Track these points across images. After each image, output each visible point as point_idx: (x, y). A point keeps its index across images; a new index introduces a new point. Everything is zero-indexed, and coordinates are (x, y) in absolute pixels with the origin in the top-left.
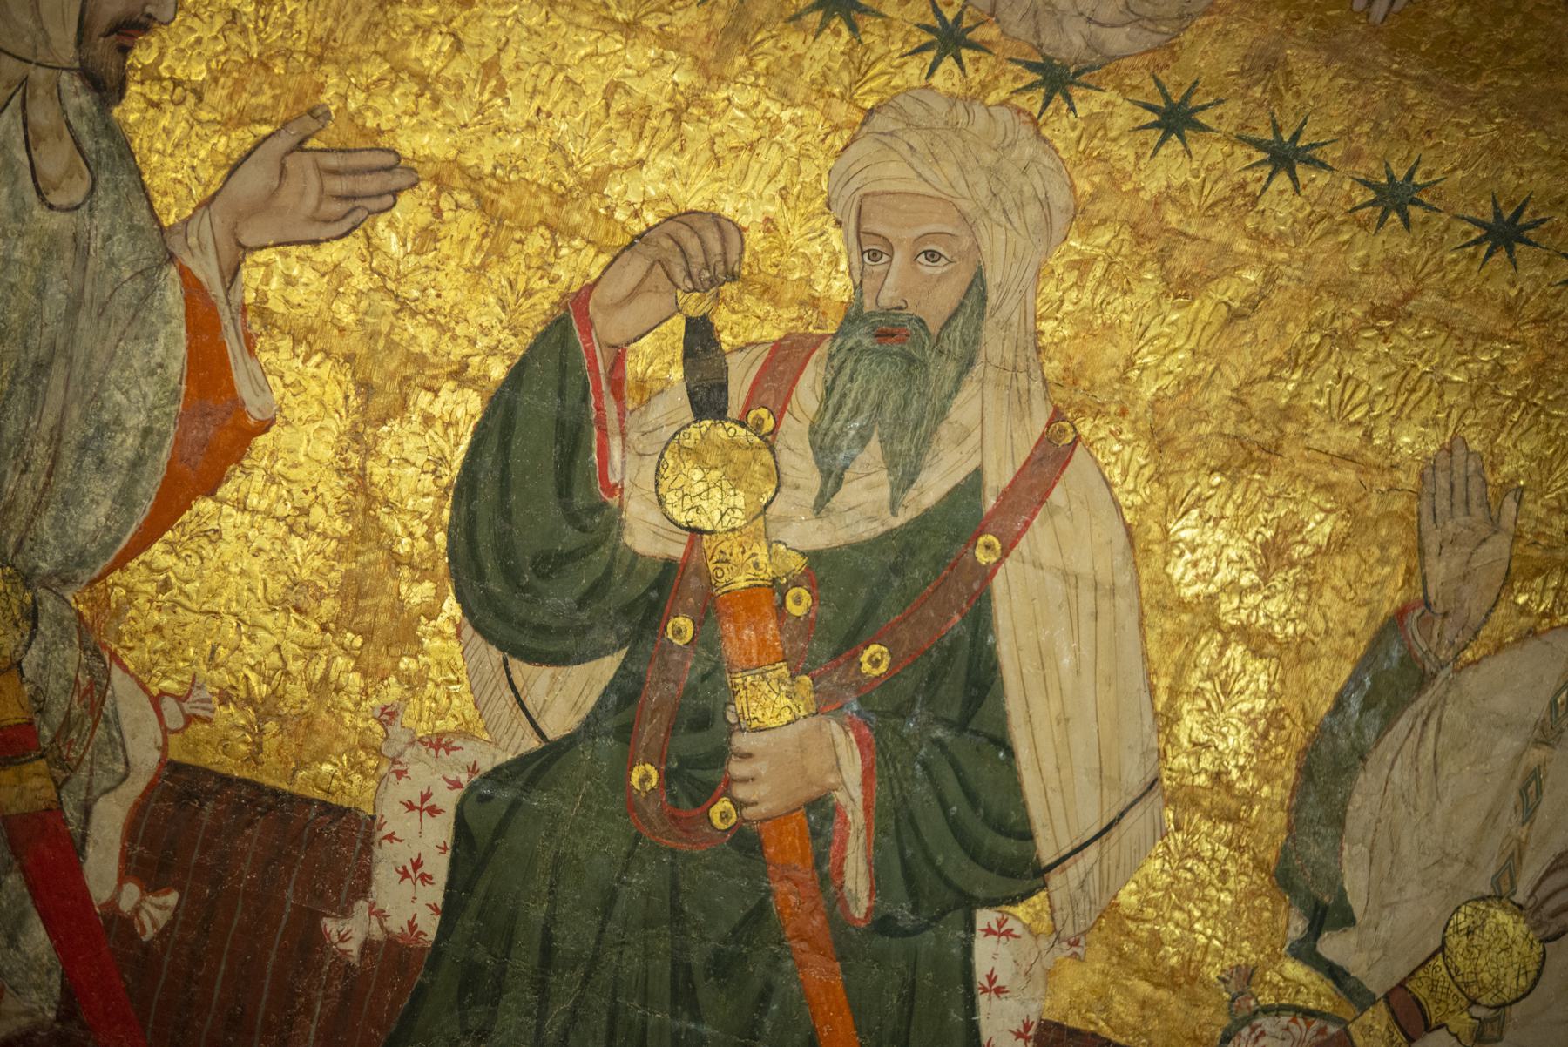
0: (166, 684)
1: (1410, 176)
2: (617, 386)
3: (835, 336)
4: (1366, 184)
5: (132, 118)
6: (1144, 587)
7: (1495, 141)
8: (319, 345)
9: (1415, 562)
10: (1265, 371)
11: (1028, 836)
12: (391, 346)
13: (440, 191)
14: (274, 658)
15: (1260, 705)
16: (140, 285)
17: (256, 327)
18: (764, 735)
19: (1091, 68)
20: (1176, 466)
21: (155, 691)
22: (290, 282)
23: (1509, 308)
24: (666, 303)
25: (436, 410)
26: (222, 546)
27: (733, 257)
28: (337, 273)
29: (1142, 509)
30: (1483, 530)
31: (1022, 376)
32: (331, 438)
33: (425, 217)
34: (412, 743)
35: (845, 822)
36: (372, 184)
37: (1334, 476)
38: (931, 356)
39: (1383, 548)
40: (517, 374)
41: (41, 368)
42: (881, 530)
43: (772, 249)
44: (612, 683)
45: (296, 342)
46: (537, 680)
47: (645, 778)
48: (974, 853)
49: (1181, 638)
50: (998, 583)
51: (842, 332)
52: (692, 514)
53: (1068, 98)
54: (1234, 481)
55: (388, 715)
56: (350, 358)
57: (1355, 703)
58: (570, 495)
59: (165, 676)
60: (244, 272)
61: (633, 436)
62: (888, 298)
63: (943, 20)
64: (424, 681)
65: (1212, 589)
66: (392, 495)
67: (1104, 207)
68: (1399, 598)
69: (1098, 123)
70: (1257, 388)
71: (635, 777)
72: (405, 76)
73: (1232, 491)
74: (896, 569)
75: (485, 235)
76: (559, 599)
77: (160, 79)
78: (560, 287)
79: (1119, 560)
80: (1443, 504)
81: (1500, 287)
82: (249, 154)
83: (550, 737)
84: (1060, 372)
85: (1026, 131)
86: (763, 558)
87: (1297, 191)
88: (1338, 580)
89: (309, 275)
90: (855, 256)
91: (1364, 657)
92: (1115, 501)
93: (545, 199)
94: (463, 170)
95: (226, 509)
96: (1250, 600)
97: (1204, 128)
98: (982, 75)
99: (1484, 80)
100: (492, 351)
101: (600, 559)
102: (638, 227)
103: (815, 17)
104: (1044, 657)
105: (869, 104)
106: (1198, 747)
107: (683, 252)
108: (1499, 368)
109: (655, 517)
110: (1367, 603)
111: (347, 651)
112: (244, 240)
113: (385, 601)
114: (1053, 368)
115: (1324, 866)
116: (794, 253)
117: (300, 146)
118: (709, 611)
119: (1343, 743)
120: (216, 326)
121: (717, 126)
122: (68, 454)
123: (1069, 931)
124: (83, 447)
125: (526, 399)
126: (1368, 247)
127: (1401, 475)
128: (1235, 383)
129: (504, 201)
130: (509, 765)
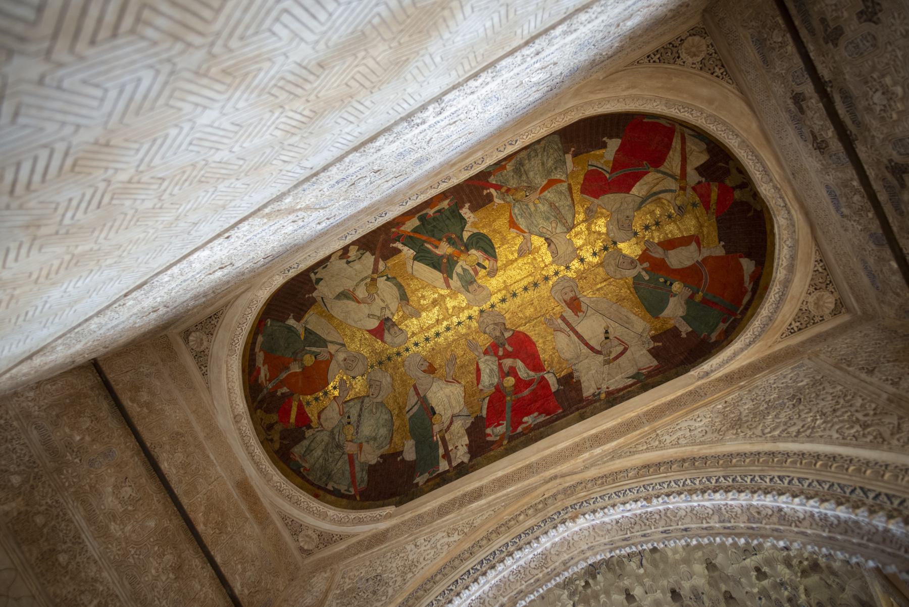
2: (487, 259)
40: (495, 251)
46: (469, 234)
69: (475, 311)
118: (462, 251)
126: (445, 323)
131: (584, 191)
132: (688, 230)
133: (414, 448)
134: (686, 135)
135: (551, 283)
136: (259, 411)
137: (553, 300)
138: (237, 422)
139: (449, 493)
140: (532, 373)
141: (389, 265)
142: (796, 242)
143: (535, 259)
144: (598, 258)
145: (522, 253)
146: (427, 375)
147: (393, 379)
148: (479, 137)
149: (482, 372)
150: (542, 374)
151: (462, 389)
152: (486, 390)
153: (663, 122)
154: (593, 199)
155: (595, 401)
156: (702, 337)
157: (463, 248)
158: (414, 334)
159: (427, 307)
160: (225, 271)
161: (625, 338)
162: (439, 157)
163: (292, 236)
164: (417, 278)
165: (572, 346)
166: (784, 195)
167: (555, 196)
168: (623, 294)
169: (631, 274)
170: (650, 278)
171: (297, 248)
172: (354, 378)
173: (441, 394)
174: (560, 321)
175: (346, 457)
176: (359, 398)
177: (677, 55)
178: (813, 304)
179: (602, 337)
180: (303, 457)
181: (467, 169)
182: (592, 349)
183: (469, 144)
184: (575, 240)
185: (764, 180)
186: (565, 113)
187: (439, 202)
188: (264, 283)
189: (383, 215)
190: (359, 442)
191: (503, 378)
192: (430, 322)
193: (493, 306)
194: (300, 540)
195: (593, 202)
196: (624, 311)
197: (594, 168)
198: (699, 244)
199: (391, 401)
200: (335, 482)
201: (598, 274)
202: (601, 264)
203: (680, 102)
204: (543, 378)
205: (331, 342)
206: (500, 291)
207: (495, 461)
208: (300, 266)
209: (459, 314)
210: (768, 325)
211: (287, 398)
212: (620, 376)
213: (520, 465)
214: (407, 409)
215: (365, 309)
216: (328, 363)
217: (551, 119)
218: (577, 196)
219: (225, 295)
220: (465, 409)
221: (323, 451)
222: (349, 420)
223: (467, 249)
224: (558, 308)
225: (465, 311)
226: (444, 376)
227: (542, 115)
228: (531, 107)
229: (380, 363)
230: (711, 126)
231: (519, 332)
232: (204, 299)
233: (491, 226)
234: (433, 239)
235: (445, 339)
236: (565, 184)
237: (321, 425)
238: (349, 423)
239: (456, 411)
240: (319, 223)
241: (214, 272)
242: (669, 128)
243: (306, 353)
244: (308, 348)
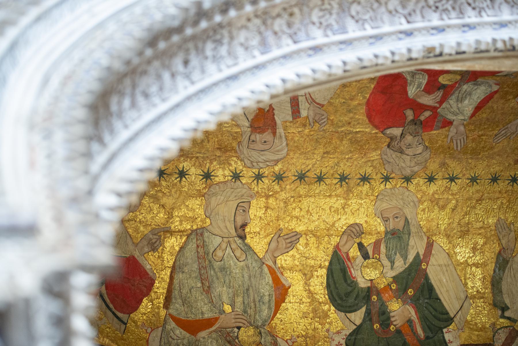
0: (287, 338)
1: (475, 175)
2: (349, 259)
3: (384, 237)
4: (468, 179)
5: (249, 241)
6: (454, 263)
7: (487, 164)
8: (294, 270)
9: (499, 242)
10: (462, 218)
11: (447, 313)
12: (307, 266)
13: (306, 236)
14: (305, 327)
15: (481, 276)
16: (260, 270)
17: (282, 270)
18: (395, 312)
19: (413, 175)
20: (452, 239)
21: (286, 340)
22: (285, 260)
23: (500, 192)
24: (352, 242)
25: (318, 274)
26: (289, 311)
27: (362, 230)
28: (293, 256)
29: (449, 249)
30: (509, 232)
31: (420, 233)
32: (302, 285)
33: (305, 241)
34: (333, 334)
35: (415, 322)
36: (294, 238)
37: (480, 232)
38: (402, 235)
39: (493, 241)
40: (331, 263)
41: (248, 290)
42: (404, 269)
43: (368, 226)
44: (365, 312)
45: (290, 271)
46: (352, 316)
47: (377, 326)
48: (439, 320)
49: (463, 269)
50: (428, 271)
51: (385, 236)
52: (370, 277)
53: (411, 182)
54: (463, 239)
55: (328, 331)
56: (300, 270)
57: (497, 270)
58: (347, 281)
59: (286, 336)
60: (277, 261)
61: (355, 267)
62: (391, 228)
63: (384, 176)
64: (332, 322)
65: (466, 259)
66: (316, 292)
67: (424, 199)
68: (498, 249)
69: (418, 184)
70: (461, 221)
71: (375, 327)
72: (293, 218)
73: (463, 240)
74: (409, 275)
75: (317, 241)
76: (351, 300)
77: (252, 233)
78: (333, 245)
79: (448, 260)
80: (500, 230)
81: (497, 189)
82: (271, 241)
83: (358, 325)
84: (426, 230)
85: (406, 190)
86: (385, 281)
87: (456, 184)
88: (487, 250)
89: (288, 258)
90: (383, 222)
91: (496, 261)
92: (444, 249)
93: (325, 231)
94: (309, 231)
95: (287, 304)
96: (473, 258)
97: (436, 179)
98: (394, 183)
99: (481, 154)
100: (325, 261)
101: (356, 291)
102: (343, 230)
103: (362, 183)
104: (440, 281)
105: (376, 195)
106: (472, 288)
107: (353, 232)
108: (502, 203)
109: (363, 280)
110: (493, 252)
111: (317, 322)
112: (275, 256)
113: (321, 311)
114: (425, 230)
115: (501, 300)
116: (372, 225)
117: (279, 236)
118: (378, 293)
119: (497, 278)
120: (275, 272)
121: (351, 208)
122: (257, 303)
123: (460, 328)
124: (259, 301)
125: (334, 267)
126: (472, 190)
127: (492, 227)
128: (457, 221)
129: (318, 234)
130: (352, 332)
144: (181, 166)
149: (475, 104)
154: (141, 260)
157: (374, 298)
167: (196, 301)
174: (304, 113)
184: (201, 212)
193: (387, 179)
209: (443, 193)
223: (370, 291)
231: (376, 127)
234: (409, 339)
236: (171, 311)
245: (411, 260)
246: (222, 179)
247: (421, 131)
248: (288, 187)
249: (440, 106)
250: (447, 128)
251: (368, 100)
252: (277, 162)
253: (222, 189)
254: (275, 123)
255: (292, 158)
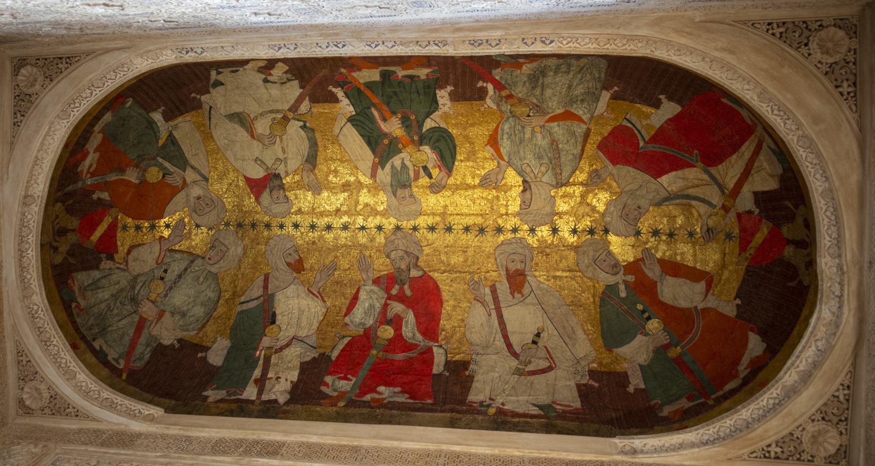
2: (439, 167)
36: (484, 182)
40: (453, 163)
41: (521, 143)
50: (373, 157)
69: (390, 224)
104: (361, 148)
118: (413, 141)
120: (499, 156)
122: (513, 133)
126: (345, 219)
131: (602, 147)
132: (705, 262)
133: (225, 352)
134: (764, 145)
135: (502, 238)
136: (59, 204)
137: (493, 260)
138: (25, 204)
139: (239, 429)
140: (419, 337)
141: (314, 110)
142: (830, 348)
143: (498, 198)
144: (576, 238)
145: (485, 182)
146: (289, 270)
147: (245, 253)
148: (509, 12)
149: (359, 302)
150: (431, 344)
151: (324, 310)
152: (352, 327)
153: (745, 114)
154: (608, 162)
155: (479, 413)
156: (653, 403)
158: (299, 211)
159: (334, 188)
160: (109, 11)
161: (557, 355)
162: (446, 10)
163: (214, 11)
164: (340, 145)
165: (487, 329)
166: (846, 283)
168: (583, 300)
169: (606, 279)
170: (627, 297)
171: (212, 30)
172: (198, 226)
173: (294, 303)
174: (487, 290)
175: (136, 318)
176: (191, 254)
177: (805, 41)
178: (809, 435)
179: (530, 338)
180: (83, 290)
181: (473, 43)
182: (509, 346)
183: (492, 14)
184: (559, 201)
185: (831, 251)
186: (631, 39)
187: (418, 66)
188: (150, 51)
189: (340, 46)
190: (162, 307)
191: (382, 323)
192: (328, 208)
193: (415, 229)
194: (26, 390)
195: (606, 167)
196: (573, 320)
197: (629, 125)
198: (709, 286)
199: (228, 279)
200: (106, 342)
201: (566, 258)
202: (576, 247)
203: (779, 100)
204: (430, 350)
205: (193, 168)
206: (434, 214)
207: (316, 420)
208: (205, 54)
209: (369, 216)
210: (741, 431)
211: (104, 207)
212: (526, 398)
213: (345, 442)
214: (243, 299)
215: (256, 149)
216: (176, 191)
217: (609, 37)
218: (591, 148)
219: (94, 41)
220: (314, 337)
221: (112, 295)
222: (163, 275)
223: (421, 142)
224: (494, 274)
225: (378, 217)
226: (309, 283)
227: (601, 26)
228: (592, 9)
229: (240, 225)
230: (801, 150)
231: (431, 278)
232: (64, 32)
233: (465, 129)
235: (335, 239)
236: (584, 127)
237: (127, 262)
238: (162, 279)
239: (302, 333)
240: (256, 14)
241: (95, 5)
242: (748, 125)
243: (155, 165)
244: (160, 160)
245: (388, 164)
246: (543, 228)
247: (395, 273)
248: (491, 222)
249: (386, 301)
250: (376, 276)
251: (442, 306)
252: (502, 244)
253: (543, 220)
254: (508, 281)
255: (491, 247)
